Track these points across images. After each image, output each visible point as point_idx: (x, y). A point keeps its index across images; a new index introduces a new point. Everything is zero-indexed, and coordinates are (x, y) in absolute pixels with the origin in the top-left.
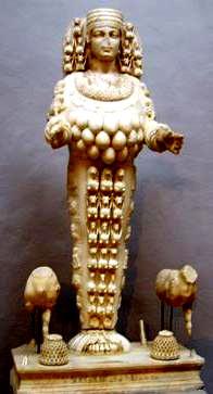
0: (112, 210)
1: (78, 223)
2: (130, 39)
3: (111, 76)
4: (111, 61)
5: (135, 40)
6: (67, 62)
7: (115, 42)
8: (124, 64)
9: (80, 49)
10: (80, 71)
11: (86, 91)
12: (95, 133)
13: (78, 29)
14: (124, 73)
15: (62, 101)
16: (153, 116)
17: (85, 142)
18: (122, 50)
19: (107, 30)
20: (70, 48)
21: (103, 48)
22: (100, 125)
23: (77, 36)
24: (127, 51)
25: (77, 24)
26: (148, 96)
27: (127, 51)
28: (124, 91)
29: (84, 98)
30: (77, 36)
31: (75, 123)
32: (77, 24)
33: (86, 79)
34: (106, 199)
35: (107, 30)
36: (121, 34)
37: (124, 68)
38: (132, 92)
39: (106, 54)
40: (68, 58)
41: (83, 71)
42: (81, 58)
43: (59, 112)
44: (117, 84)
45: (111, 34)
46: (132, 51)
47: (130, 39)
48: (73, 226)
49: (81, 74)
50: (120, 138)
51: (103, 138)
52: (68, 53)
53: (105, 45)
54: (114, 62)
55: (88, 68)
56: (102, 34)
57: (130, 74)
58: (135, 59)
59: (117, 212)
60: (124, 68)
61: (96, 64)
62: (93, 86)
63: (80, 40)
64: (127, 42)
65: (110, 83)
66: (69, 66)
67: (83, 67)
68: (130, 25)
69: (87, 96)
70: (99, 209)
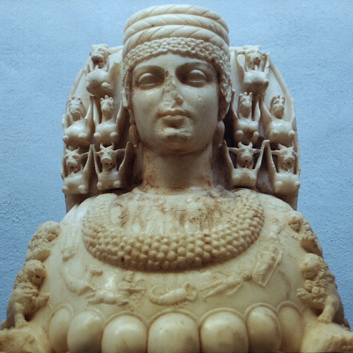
2: (257, 90)
3: (192, 200)
4: (197, 153)
5: (273, 91)
6: (68, 169)
8: (238, 161)
9: (108, 127)
10: (111, 190)
13: (102, 74)
14: (239, 186)
16: (328, 310)
18: (230, 122)
19: (170, 63)
20: (79, 129)
21: (160, 115)
23: (97, 91)
24: (245, 123)
25: (97, 62)
27: (245, 123)
28: (221, 231)
29: (96, 265)
30: (97, 91)
32: (97, 62)
33: (116, 212)
36: (216, 74)
37: (237, 173)
38: (252, 238)
39: (170, 131)
40: (72, 155)
41: (118, 191)
42: (107, 153)
43: (28, 317)
44: (207, 217)
45: (184, 75)
46: (264, 123)
47: (257, 90)
49: (111, 197)
52: (72, 142)
53: (167, 106)
54: (208, 154)
55: (131, 181)
56: (157, 77)
57: (260, 189)
58: (274, 146)
60: (237, 173)
61: (151, 166)
63: (106, 103)
64: (247, 100)
65: (182, 219)
66: (77, 178)
67: (115, 177)
68: (254, 50)
69: (106, 258)
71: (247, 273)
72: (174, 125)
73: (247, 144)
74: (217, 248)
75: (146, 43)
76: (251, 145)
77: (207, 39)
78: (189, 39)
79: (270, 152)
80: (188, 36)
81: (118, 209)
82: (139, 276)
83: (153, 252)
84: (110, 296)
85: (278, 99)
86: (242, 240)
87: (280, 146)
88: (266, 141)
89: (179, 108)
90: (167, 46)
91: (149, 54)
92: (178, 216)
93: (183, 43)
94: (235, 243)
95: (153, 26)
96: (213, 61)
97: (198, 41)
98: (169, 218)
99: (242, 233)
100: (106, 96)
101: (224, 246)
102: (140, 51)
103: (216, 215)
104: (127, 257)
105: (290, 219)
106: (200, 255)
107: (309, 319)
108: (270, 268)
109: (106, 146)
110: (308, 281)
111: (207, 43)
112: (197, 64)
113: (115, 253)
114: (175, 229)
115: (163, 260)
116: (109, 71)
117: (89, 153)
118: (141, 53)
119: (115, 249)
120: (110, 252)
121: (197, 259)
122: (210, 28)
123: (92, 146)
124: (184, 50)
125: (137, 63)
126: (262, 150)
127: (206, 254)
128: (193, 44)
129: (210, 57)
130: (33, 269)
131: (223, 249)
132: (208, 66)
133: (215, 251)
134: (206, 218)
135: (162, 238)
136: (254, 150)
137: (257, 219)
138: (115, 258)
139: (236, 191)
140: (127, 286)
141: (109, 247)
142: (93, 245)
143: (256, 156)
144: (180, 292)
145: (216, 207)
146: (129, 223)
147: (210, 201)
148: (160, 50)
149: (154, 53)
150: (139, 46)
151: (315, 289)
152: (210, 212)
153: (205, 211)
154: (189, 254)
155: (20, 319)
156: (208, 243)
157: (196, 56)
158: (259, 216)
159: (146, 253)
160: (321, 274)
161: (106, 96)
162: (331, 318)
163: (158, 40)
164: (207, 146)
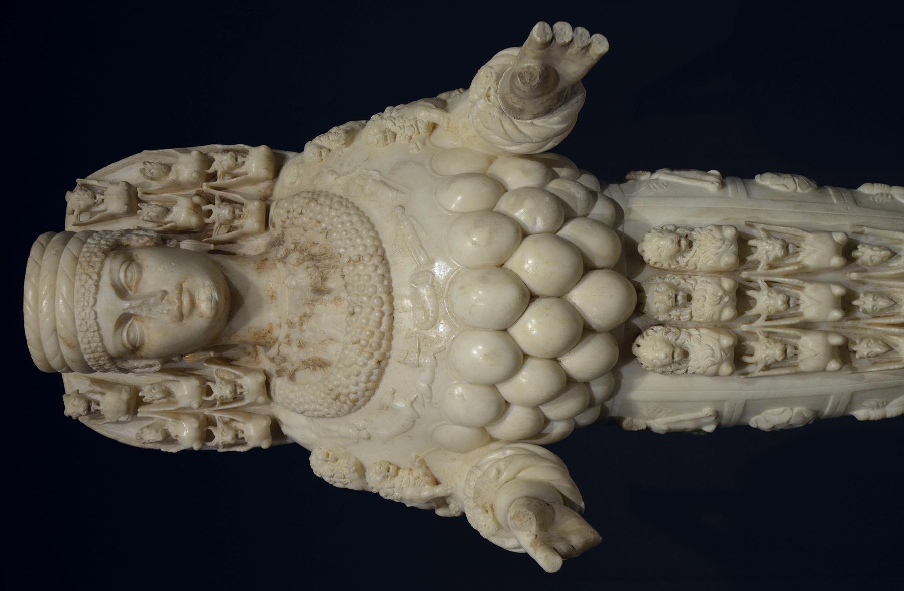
0: (806, 274)
1: (853, 399)
7: (155, 274)
9: (185, 390)
11: (353, 387)
12: (521, 358)
15: (391, 470)
17: (552, 398)
21: (181, 317)
22: (495, 342)
26: (351, 135)
27: (182, 215)
31: (483, 429)
34: (765, 301)
35: (108, 305)
43: (437, 482)
48: (861, 414)
50: (534, 264)
51: (537, 328)
59: (815, 252)
62: (332, 352)
65: (320, 291)
70: (806, 326)
71: (399, 212)
72: (193, 304)
73: (210, 213)
74: (365, 246)
75: (80, 340)
76: (210, 207)
77: (76, 259)
78: (77, 283)
79: (219, 182)
80: (73, 283)
81: (299, 375)
82: (399, 342)
83: (372, 325)
84: (426, 375)
85: (147, 171)
86: (355, 219)
87: (211, 171)
88: (205, 187)
89: (173, 295)
90: (88, 312)
91: (96, 334)
92: (318, 297)
93: (83, 290)
94: (358, 226)
95: (55, 330)
96: (106, 253)
97: (80, 271)
98: (319, 308)
99: (344, 217)
100: (140, 394)
101: (362, 238)
102: (90, 348)
103: (315, 250)
104: (377, 355)
105: (317, 158)
106: (376, 267)
107: (444, 139)
108: (385, 184)
109: (209, 392)
110: (397, 139)
111: (81, 259)
112: (111, 272)
113: (371, 374)
114: (337, 299)
115: (383, 314)
116: (104, 391)
117: (217, 415)
118: (94, 345)
119: (365, 371)
120: (368, 380)
121: (379, 271)
122: (59, 254)
123: (207, 412)
124: (93, 289)
125: (105, 351)
126: (217, 193)
127: (376, 260)
128: (84, 277)
129: (102, 255)
130: (378, 478)
131: (368, 242)
132: (115, 257)
133: (371, 250)
134: (319, 261)
135: (353, 314)
136: (217, 202)
137: (322, 200)
138: (376, 371)
139: (274, 226)
140: (413, 357)
141: (363, 378)
142: (354, 402)
143: (224, 200)
144: (425, 292)
145: (302, 251)
146: (325, 357)
147: (294, 257)
148: (91, 322)
149: (96, 328)
150: (83, 347)
151: (409, 132)
152: (313, 257)
153: (310, 263)
154: (375, 280)
155: (439, 491)
156: (360, 258)
157: (100, 276)
158: (315, 196)
159: (372, 333)
160: (389, 124)
161: (140, 394)
162: (445, 115)
163: (78, 323)
164: (216, 263)
